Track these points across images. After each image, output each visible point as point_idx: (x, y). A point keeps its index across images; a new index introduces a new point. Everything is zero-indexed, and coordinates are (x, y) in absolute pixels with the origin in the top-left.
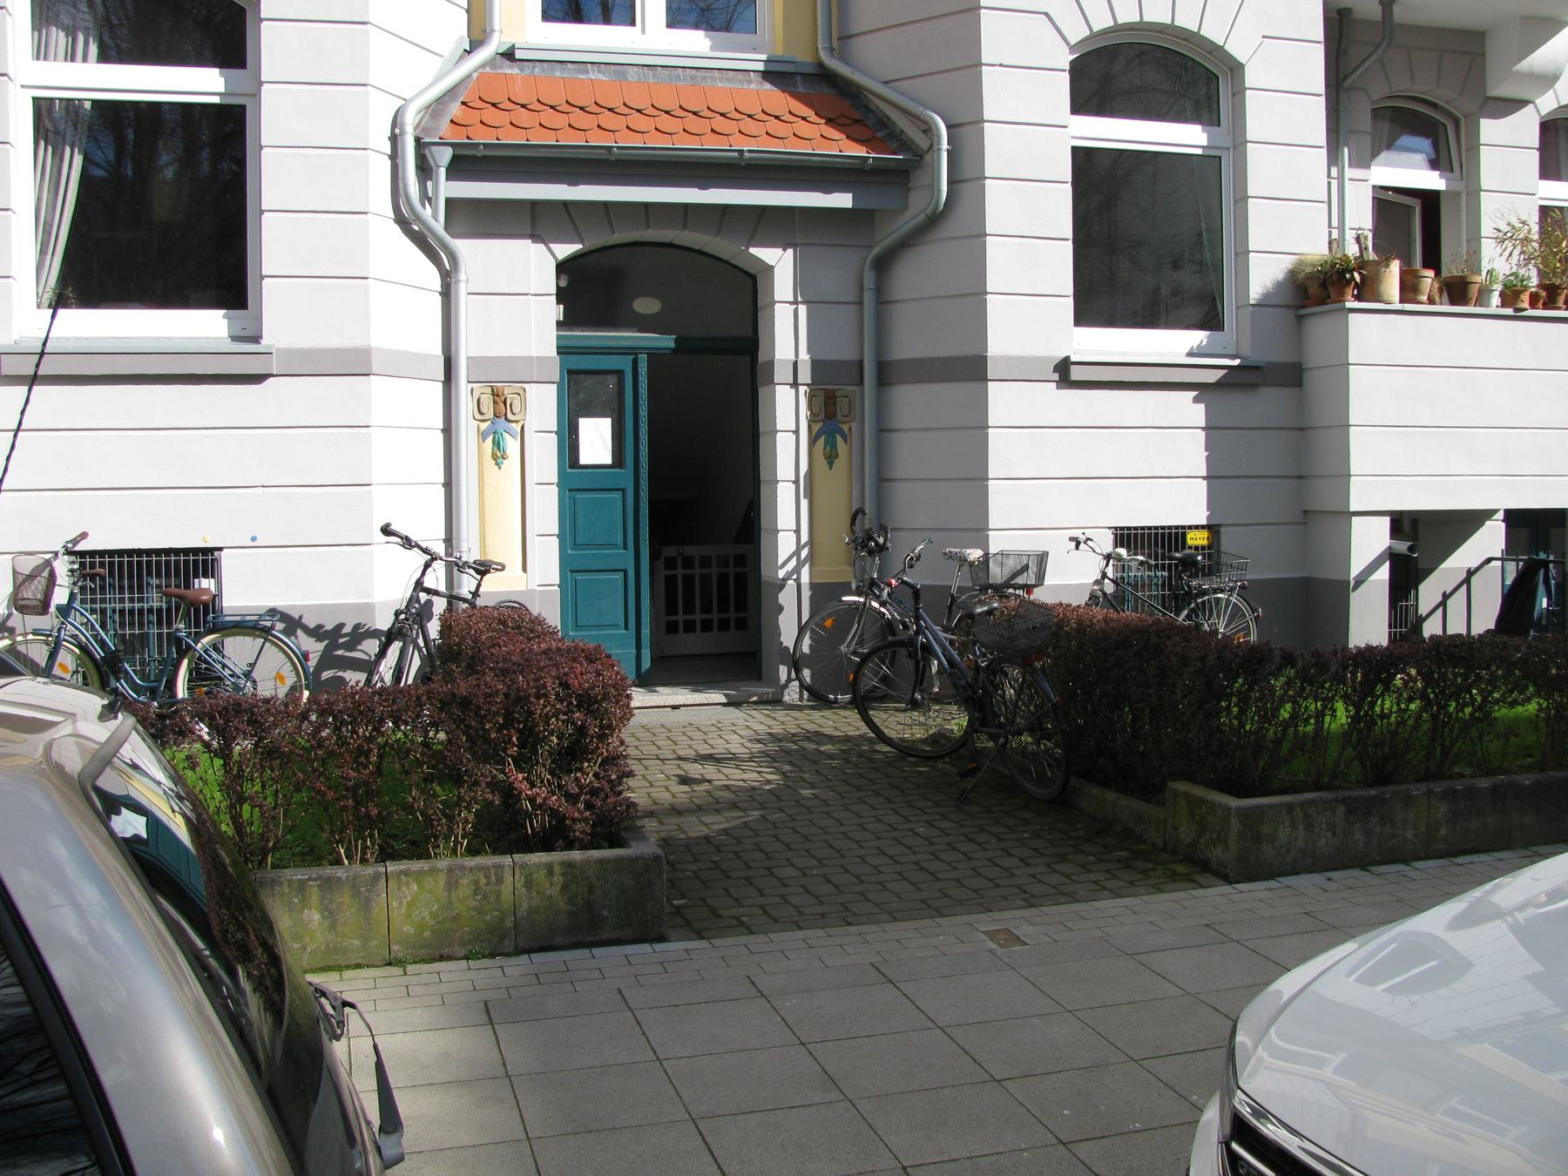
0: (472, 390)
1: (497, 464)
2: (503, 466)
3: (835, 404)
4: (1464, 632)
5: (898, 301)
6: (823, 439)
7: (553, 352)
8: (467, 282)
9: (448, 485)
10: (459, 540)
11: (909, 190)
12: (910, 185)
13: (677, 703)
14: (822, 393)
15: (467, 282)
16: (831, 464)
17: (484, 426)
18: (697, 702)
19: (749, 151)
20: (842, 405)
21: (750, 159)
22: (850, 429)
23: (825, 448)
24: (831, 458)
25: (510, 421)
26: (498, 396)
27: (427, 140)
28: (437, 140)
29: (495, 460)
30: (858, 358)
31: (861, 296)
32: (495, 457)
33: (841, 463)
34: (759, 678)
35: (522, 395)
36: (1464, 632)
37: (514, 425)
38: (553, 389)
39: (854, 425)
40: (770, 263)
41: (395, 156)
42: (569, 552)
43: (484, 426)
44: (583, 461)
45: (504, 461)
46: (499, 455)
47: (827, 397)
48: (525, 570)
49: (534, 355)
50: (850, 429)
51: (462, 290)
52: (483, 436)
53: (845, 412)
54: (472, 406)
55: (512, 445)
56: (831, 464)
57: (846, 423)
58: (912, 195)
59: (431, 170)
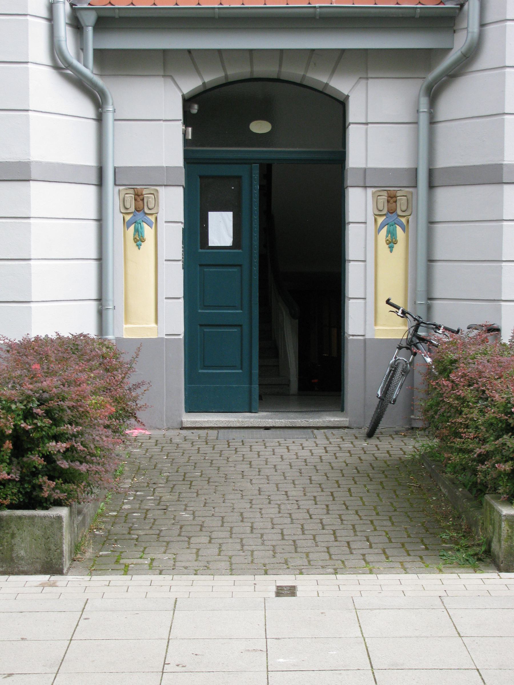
0: (119, 191)
1: (137, 245)
2: (141, 247)
3: (395, 202)
4: (92, 331)
5: (440, 122)
6: (385, 229)
7: (180, 162)
8: (114, 111)
9: (100, 259)
10: (107, 300)
11: (454, 32)
12: (455, 28)
13: (268, 426)
14: (385, 193)
15: (114, 111)
16: (391, 248)
17: (128, 218)
18: (283, 425)
19: (320, 7)
20: (402, 203)
21: (320, 13)
22: (408, 222)
23: (387, 236)
24: (392, 243)
25: (146, 214)
26: (139, 196)
27: (79, 6)
28: (86, 6)
29: (135, 242)
30: (412, 166)
31: (418, 118)
32: (136, 240)
33: (400, 248)
34: (342, 410)
35: (156, 195)
36: (92, 331)
37: (150, 217)
38: (180, 191)
39: (411, 218)
40: (346, 93)
41: (51, 19)
42: (200, 311)
43: (128, 218)
44: (210, 244)
45: (143, 244)
46: (139, 240)
47: (389, 197)
48: (156, 322)
49: (164, 165)
50: (408, 222)
51: (109, 118)
52: (127, 224)
53: (404, 208)
54: (118, 203)
55: (148, 232)
56: (391, 248)
57: (404, 216)
58: (456, 35)
59: (82, 28)
